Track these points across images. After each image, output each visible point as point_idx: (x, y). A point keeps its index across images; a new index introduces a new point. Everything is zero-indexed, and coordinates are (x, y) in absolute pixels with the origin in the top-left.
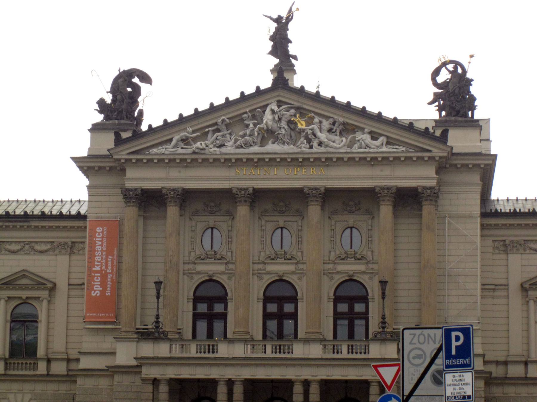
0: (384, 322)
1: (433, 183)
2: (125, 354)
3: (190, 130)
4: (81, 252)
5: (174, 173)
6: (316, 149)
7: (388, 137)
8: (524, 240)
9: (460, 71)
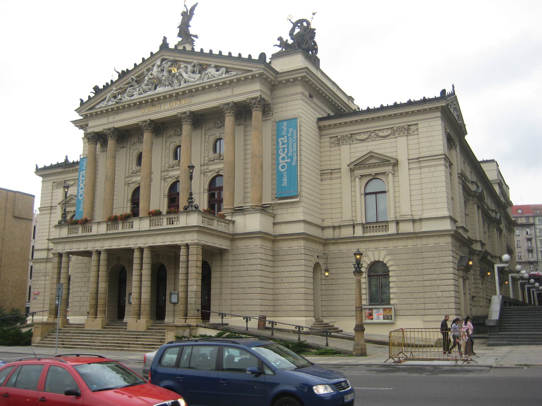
3: (114, 88)
5: (111, 119)
6: (183, 85)
8: (351, 134)
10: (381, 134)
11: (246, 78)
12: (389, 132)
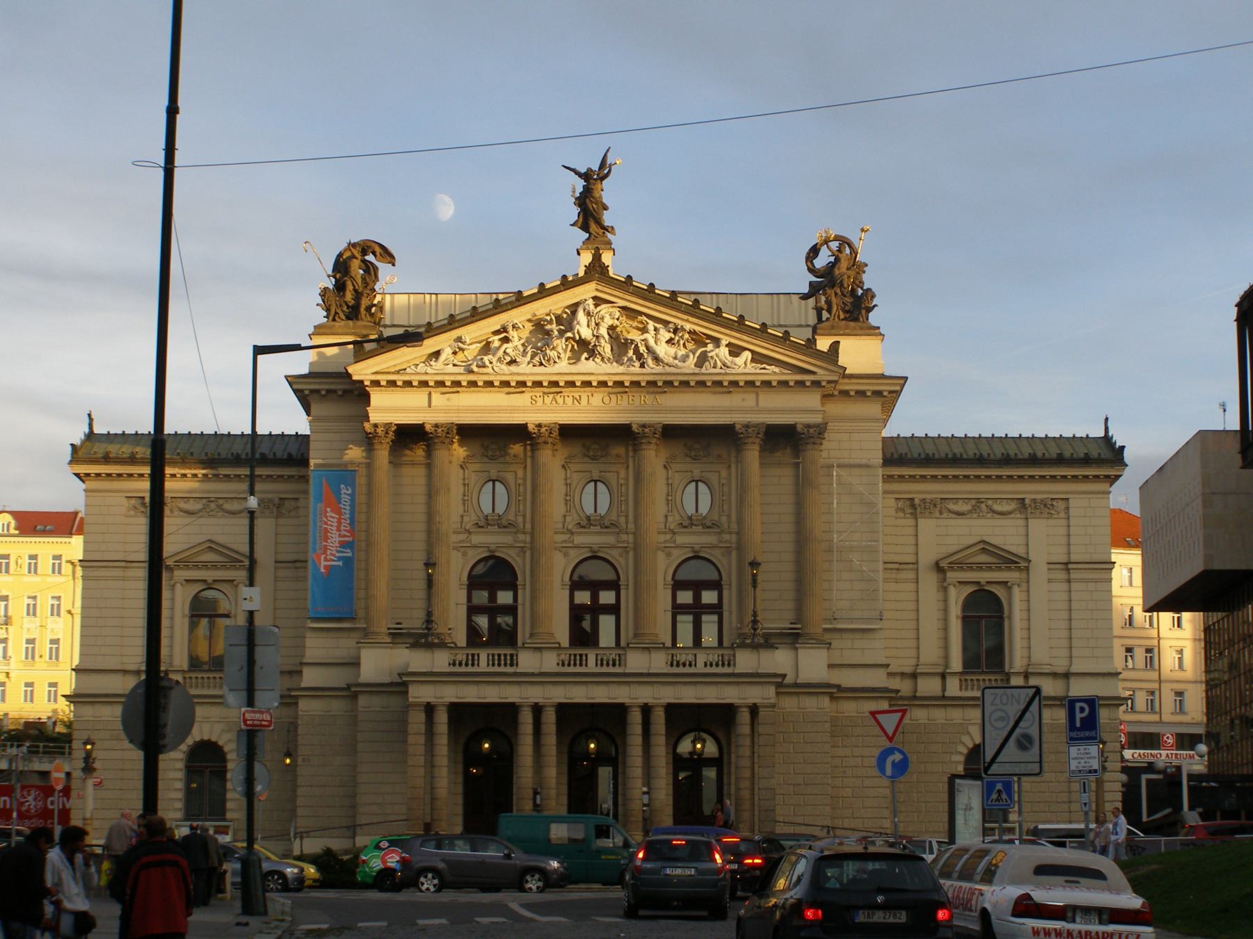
0: (755, 622)
1: (817, 419)
2: (377, 663)
4: (293, 514)
9: (848, 251)
10: (997, 507)
11: (801, 383)
12: (1013, 506)
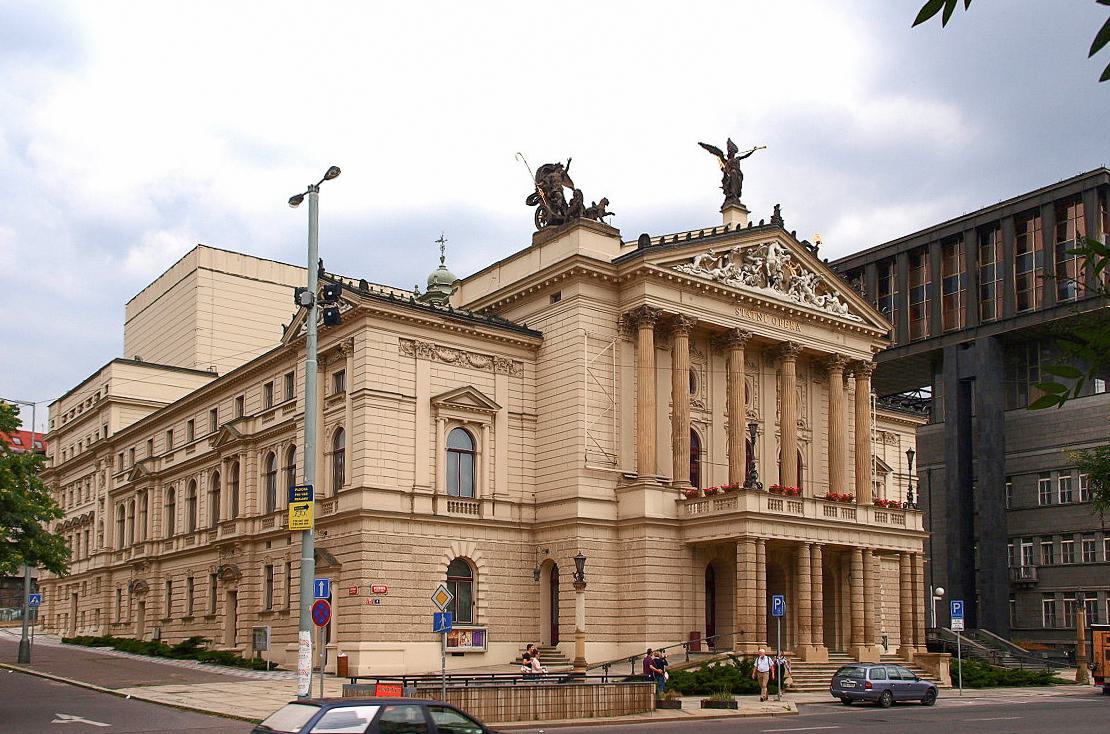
3: (713, 252)
5: (687, 299)
7: (848, 304)
11: (870, 332)
